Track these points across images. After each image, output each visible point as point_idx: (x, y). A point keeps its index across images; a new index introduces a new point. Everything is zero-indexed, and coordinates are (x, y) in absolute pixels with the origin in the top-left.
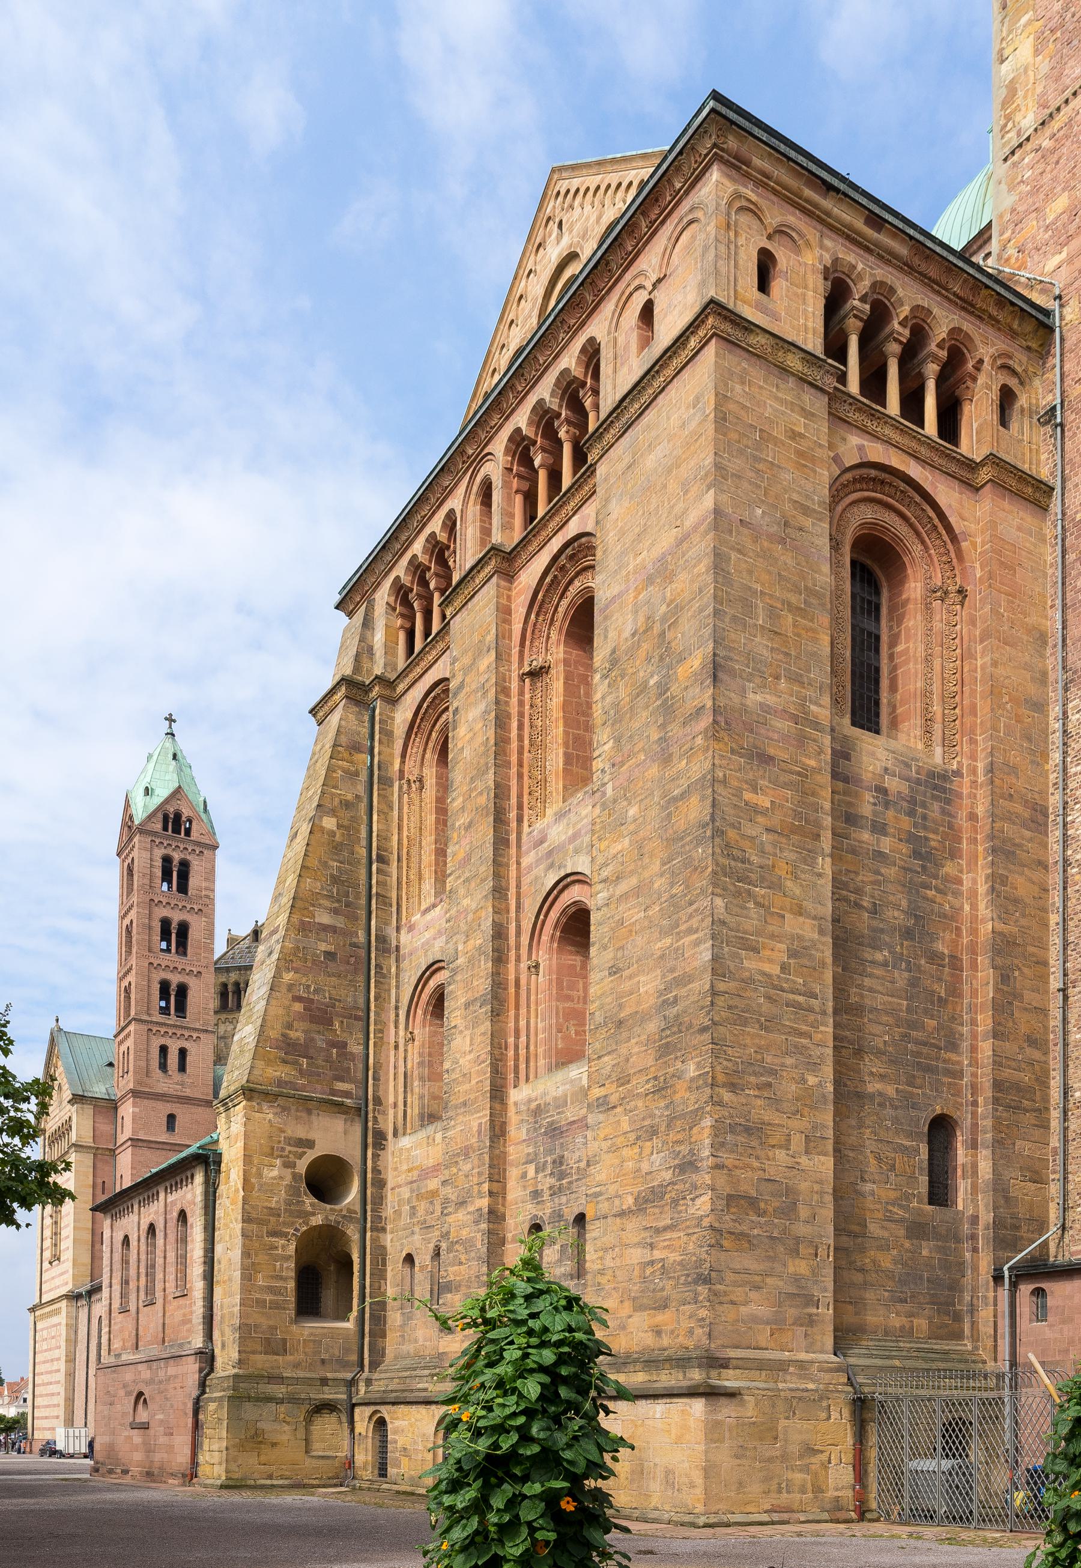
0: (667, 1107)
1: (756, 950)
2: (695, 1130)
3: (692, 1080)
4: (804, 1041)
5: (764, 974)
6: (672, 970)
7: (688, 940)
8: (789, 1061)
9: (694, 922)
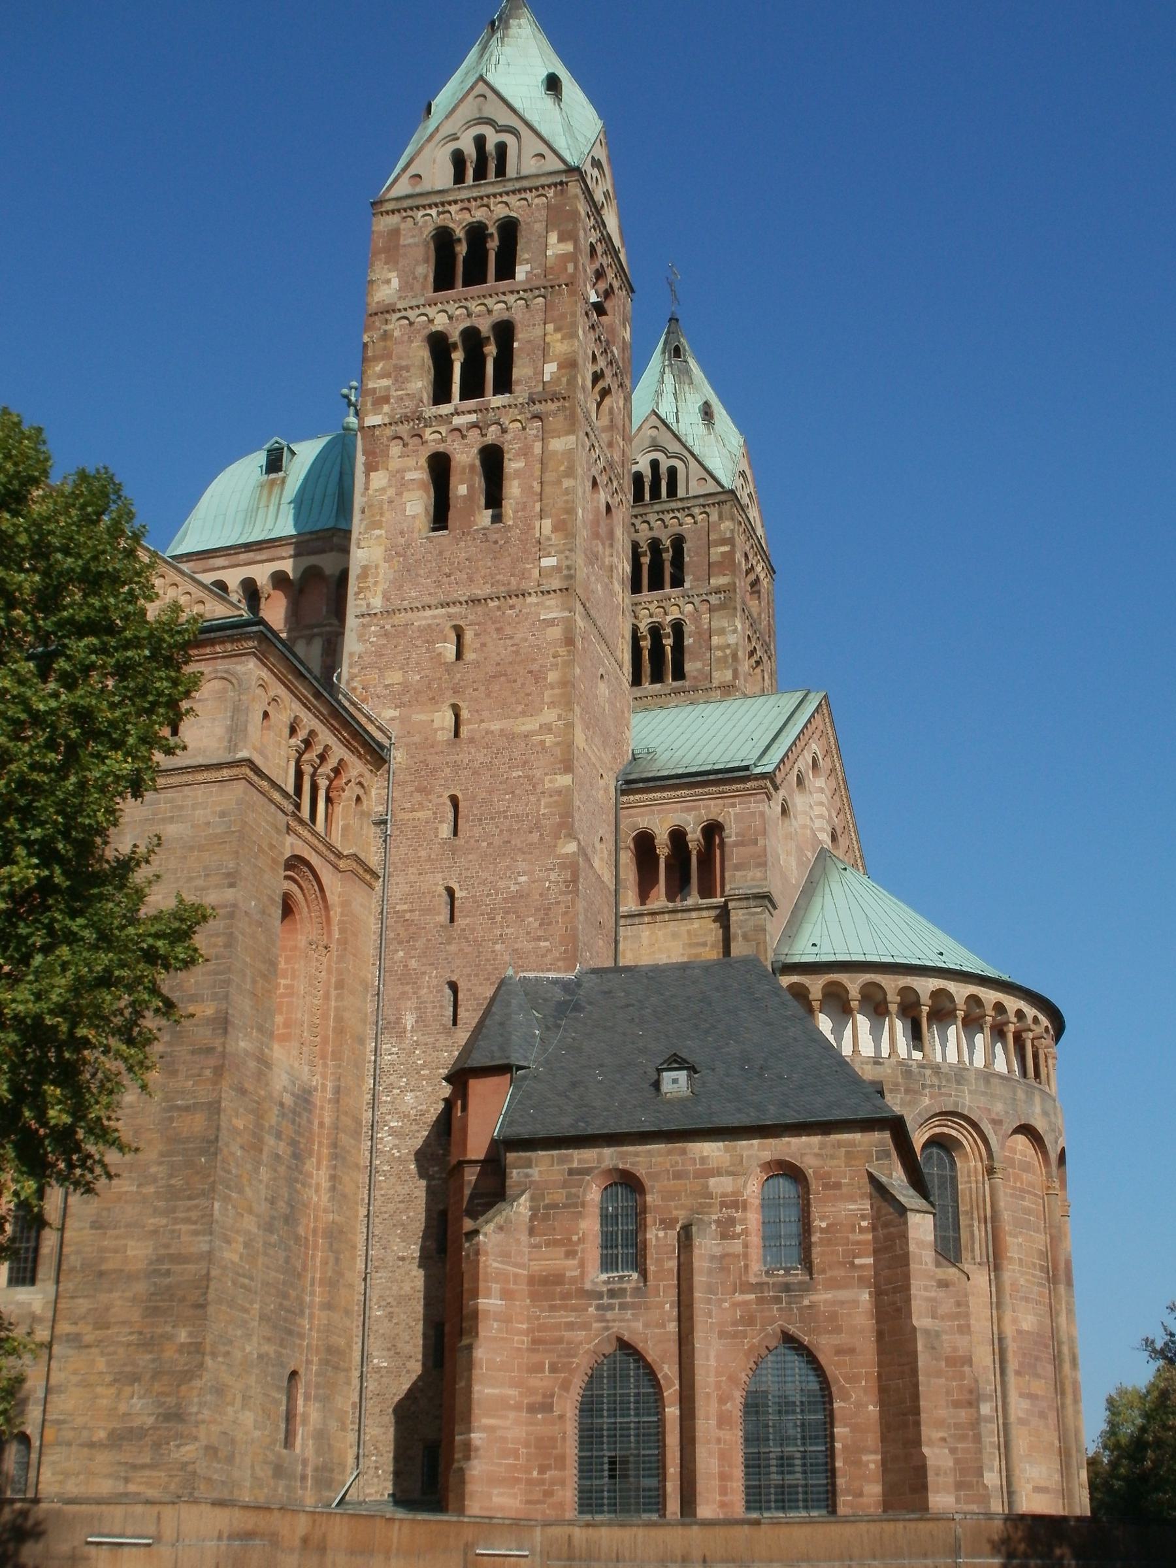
0: (154, 1360)
1: (228, 1242)
2: (183, 1388)
3: (182, 1345)
4: (245, 1316)
5: (232, 1262)
6: (167, 1246)
7: (184, 1228)
8: (239, 1333)
9: (194, 1215)
